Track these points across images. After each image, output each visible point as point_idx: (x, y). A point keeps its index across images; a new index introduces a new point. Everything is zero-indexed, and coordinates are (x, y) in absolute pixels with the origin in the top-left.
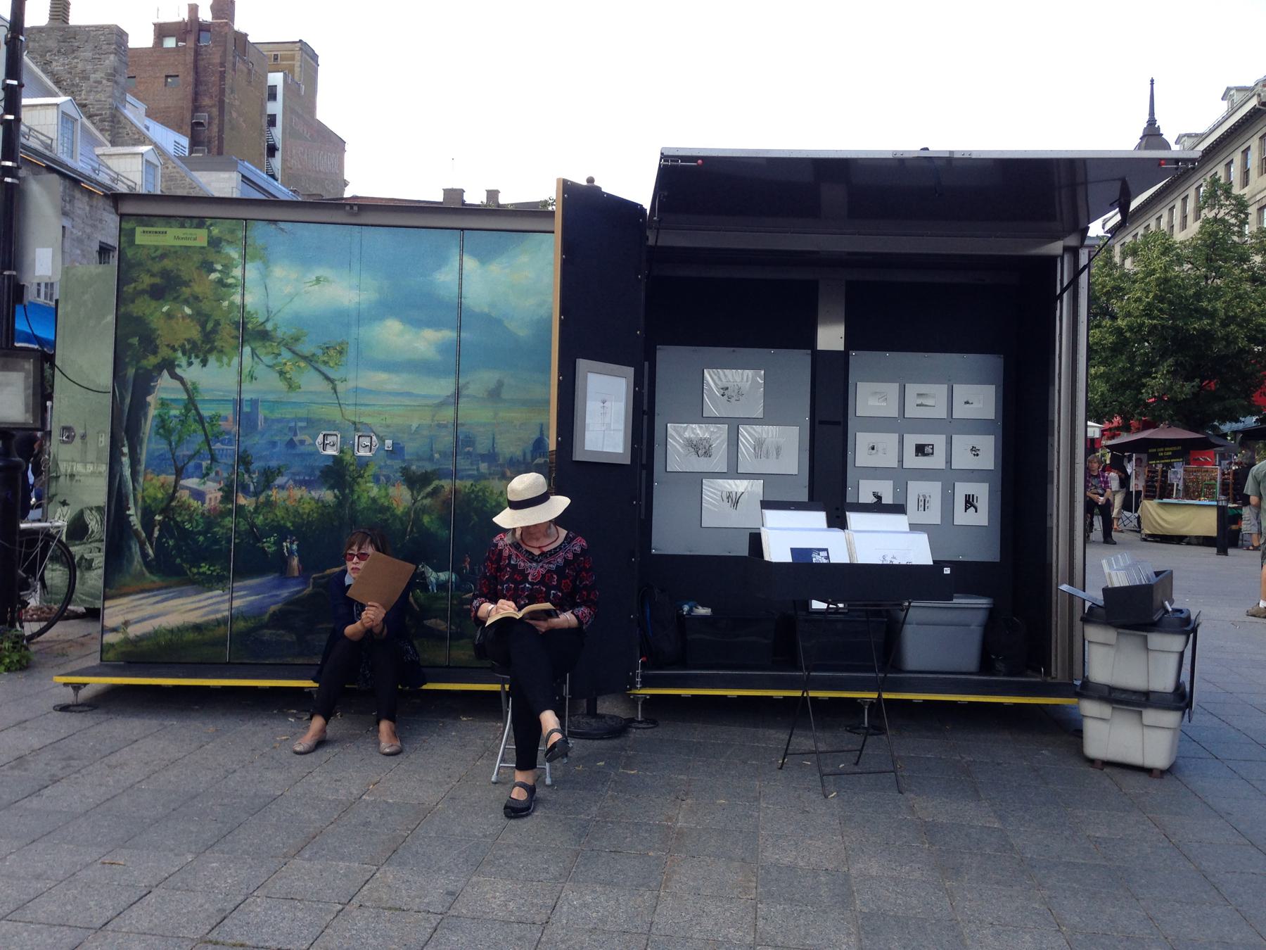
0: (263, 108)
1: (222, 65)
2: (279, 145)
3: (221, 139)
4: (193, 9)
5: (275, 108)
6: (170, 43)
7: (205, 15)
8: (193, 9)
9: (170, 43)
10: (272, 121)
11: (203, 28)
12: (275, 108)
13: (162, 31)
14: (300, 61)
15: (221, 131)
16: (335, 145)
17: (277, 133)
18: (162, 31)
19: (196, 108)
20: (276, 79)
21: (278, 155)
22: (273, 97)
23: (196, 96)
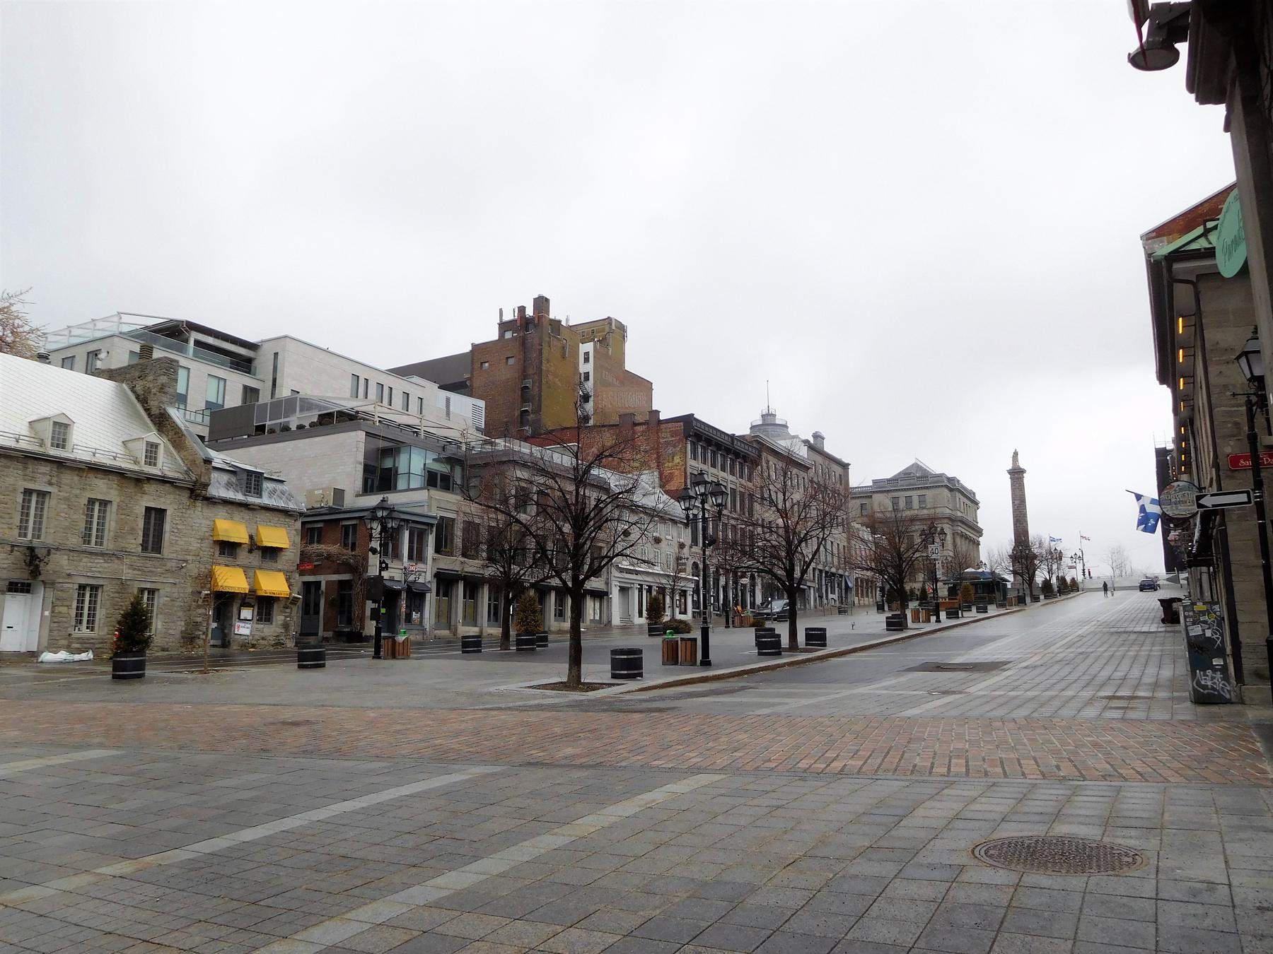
2: (591, 394)
3: (540, 396)
6: (508, 335)
7: (530, 312)
8: (522, 309)
9: (508, 335)
10: (587, 376)
14: (608, 335)
15: (540, 390)
17: (589, 385)
18: (504, 326)
19: (525, 376)
22: (586, 360)
23: (524, 369)
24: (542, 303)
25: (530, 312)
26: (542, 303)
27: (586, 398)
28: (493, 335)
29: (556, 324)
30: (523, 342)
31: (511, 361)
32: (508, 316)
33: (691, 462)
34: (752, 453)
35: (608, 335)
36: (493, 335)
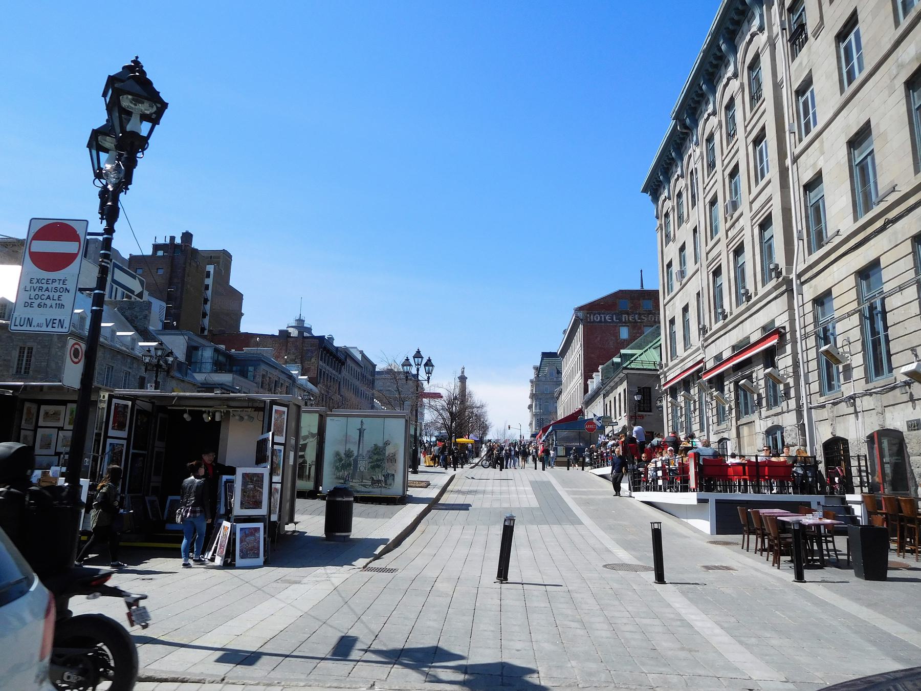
0: (203, 281)
1: (185, 264)
2: (210, 299)
4: (172, 238)
5: (209, 281)
6: (160, 253)
7: (178, 241)
8: (172, 238)
9: (160, 253)
10: (207, 287)
11: (177, 246)
12: (209, 281)
13: (156, 247)
14: (222, 259)
16: (237, 297)
17: (209, 293)
18: (156, 247)
19: (170, 284)
20: (211, 268)
21: (209, 303)
24: (187, 237)
25: (178, 241)
26: (187, 237)
27: (206, 301)
28: (148, 252)
29: (196, 251)
30: (173, 259)
31: (161, 272)
32: (161, 241)
33: (321, 363)
34: (342, 357)
35: (222, 259)
36: (148, 252)
